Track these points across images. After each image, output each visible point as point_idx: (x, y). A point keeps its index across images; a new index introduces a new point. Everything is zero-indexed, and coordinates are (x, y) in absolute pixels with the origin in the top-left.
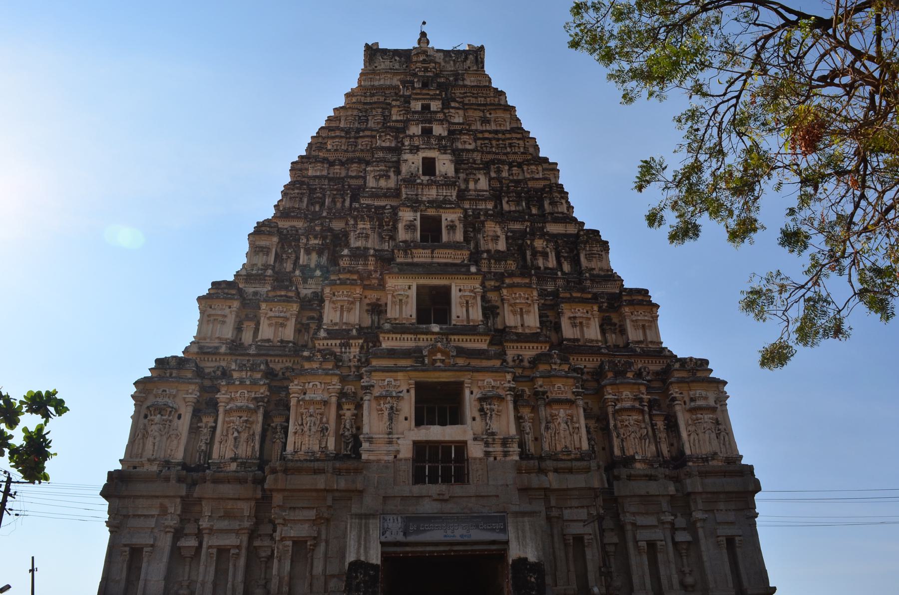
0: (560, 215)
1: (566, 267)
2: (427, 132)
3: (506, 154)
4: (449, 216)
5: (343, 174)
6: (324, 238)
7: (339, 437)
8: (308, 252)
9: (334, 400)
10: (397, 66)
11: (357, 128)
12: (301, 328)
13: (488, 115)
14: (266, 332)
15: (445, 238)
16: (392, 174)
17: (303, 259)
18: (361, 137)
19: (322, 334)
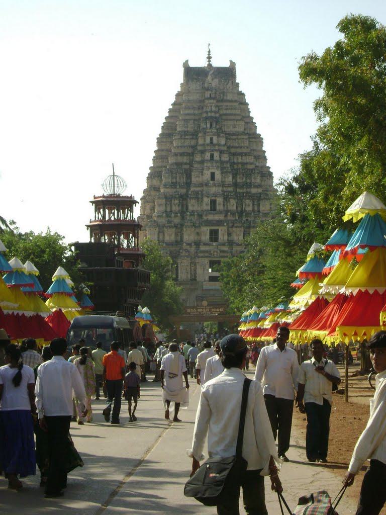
0: (257, 184)
1: (256, 208)
2: (212, 156)
3: (241, 147)
4: (220, 200)
5: (181, 161)
6: (179, 200)
7: (191, 274)
8: (175, 205)
9: (189, 265)
10: (198, 88)
11: (185, 131)
12: (176, 235)
13: (235, 123)
14: (167, 238)
15: (218, 207)
16: (200, 175)
17: (174, 208)
18: (187, 139)
19: (185, 244)
